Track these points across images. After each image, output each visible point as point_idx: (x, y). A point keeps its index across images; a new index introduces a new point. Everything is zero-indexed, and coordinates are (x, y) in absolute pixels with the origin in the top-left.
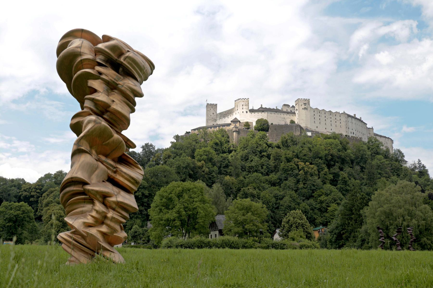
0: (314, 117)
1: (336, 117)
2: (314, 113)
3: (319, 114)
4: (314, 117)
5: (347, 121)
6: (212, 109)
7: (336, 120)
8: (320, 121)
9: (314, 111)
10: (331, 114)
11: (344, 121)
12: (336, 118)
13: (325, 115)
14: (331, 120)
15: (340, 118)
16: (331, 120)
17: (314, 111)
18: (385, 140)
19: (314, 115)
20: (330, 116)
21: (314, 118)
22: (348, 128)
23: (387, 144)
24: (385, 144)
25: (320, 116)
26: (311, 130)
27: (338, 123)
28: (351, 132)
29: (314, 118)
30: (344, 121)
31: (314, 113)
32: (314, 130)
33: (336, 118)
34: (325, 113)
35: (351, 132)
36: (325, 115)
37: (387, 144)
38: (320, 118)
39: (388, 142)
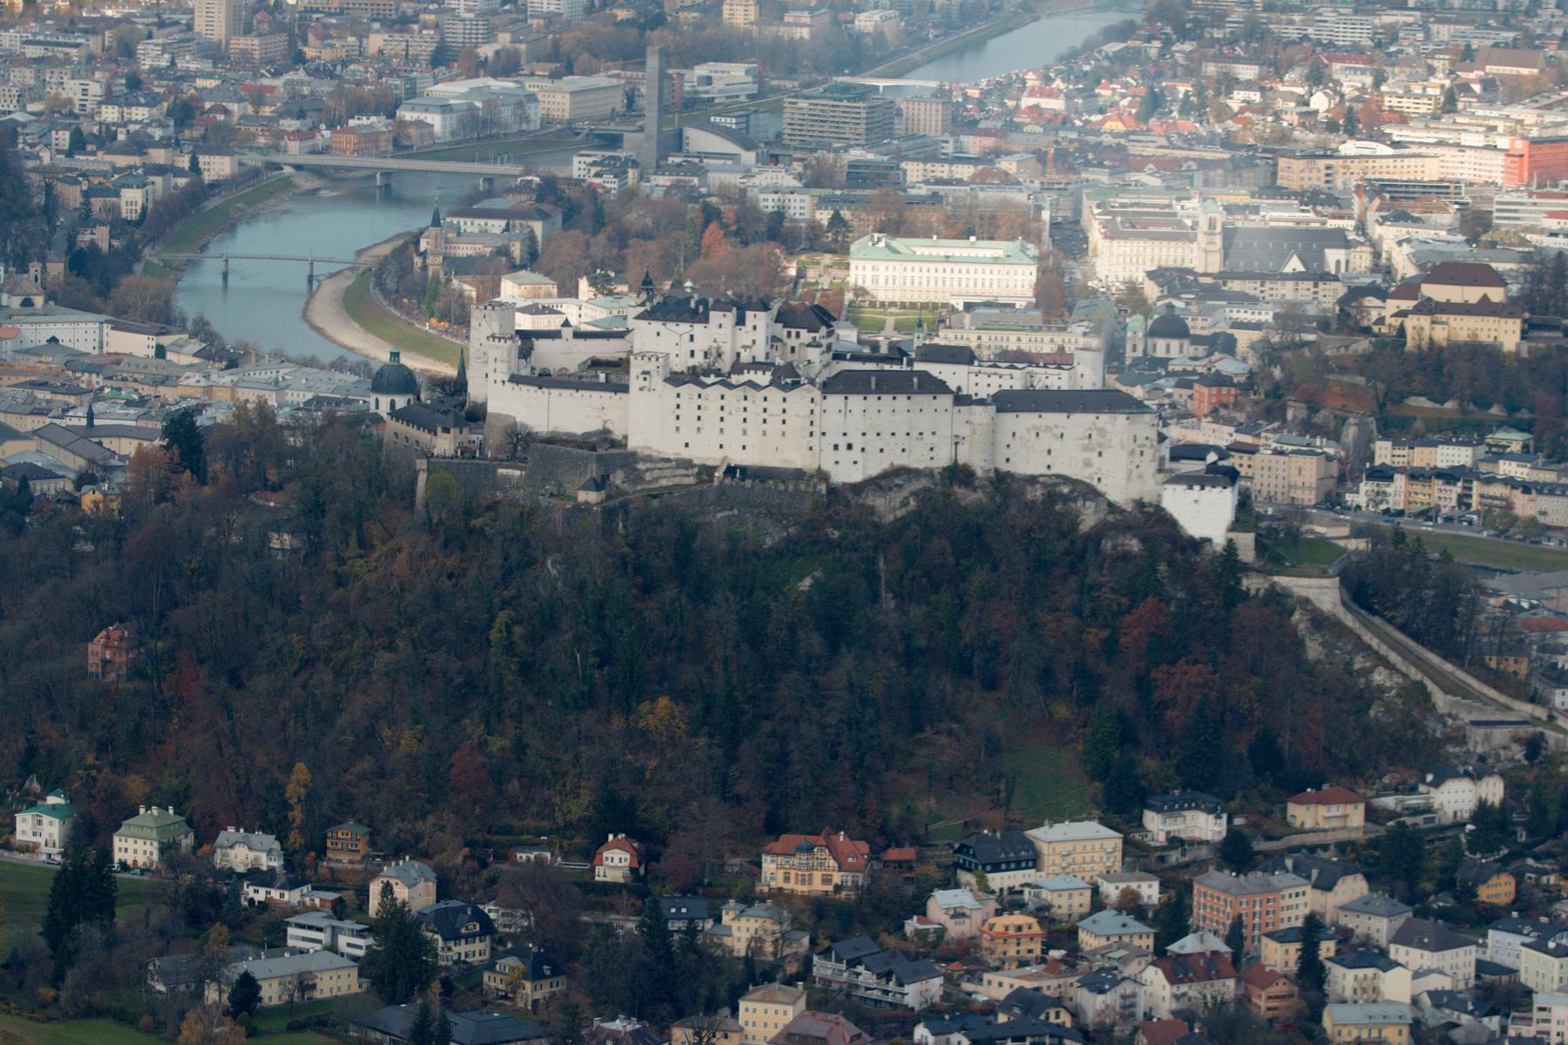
0: (678, 412)
1: (765, 405)
2: (679, 401)
3: (699, 402)
4: (678, 412)
5: (817, 412)
6: (484, 323)
7: (765, 416)
8: (699, 424)
9: (678, 395)
10: (746, 398)
11: (798, 416)
12: (765, 410)
13: (722, 403)
14: (745, 415)
15: (784, 405)
16: (745, 415)
17: (678, 395)
18: (1094, 423)
19: (678, 406)
20: (745, 404)
21: (678, 417)
22: (817, 434)
23: (1104, 437)
24: (1094, 436)
25: (699, 407)
26: (662, 456)
27: (774, 425)
28: (836, 447)
29: (678, 417)
30: (798, 416)
31: (679, 401)
32: (672, 457)
33: (765, 410)
34: (722, 397)
35: (836, 447)
36: (722, 403)
37: (1104, 437)
38: (699, 413)
39: (1108, 427)
